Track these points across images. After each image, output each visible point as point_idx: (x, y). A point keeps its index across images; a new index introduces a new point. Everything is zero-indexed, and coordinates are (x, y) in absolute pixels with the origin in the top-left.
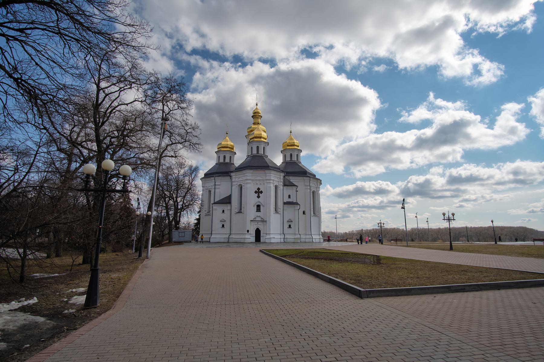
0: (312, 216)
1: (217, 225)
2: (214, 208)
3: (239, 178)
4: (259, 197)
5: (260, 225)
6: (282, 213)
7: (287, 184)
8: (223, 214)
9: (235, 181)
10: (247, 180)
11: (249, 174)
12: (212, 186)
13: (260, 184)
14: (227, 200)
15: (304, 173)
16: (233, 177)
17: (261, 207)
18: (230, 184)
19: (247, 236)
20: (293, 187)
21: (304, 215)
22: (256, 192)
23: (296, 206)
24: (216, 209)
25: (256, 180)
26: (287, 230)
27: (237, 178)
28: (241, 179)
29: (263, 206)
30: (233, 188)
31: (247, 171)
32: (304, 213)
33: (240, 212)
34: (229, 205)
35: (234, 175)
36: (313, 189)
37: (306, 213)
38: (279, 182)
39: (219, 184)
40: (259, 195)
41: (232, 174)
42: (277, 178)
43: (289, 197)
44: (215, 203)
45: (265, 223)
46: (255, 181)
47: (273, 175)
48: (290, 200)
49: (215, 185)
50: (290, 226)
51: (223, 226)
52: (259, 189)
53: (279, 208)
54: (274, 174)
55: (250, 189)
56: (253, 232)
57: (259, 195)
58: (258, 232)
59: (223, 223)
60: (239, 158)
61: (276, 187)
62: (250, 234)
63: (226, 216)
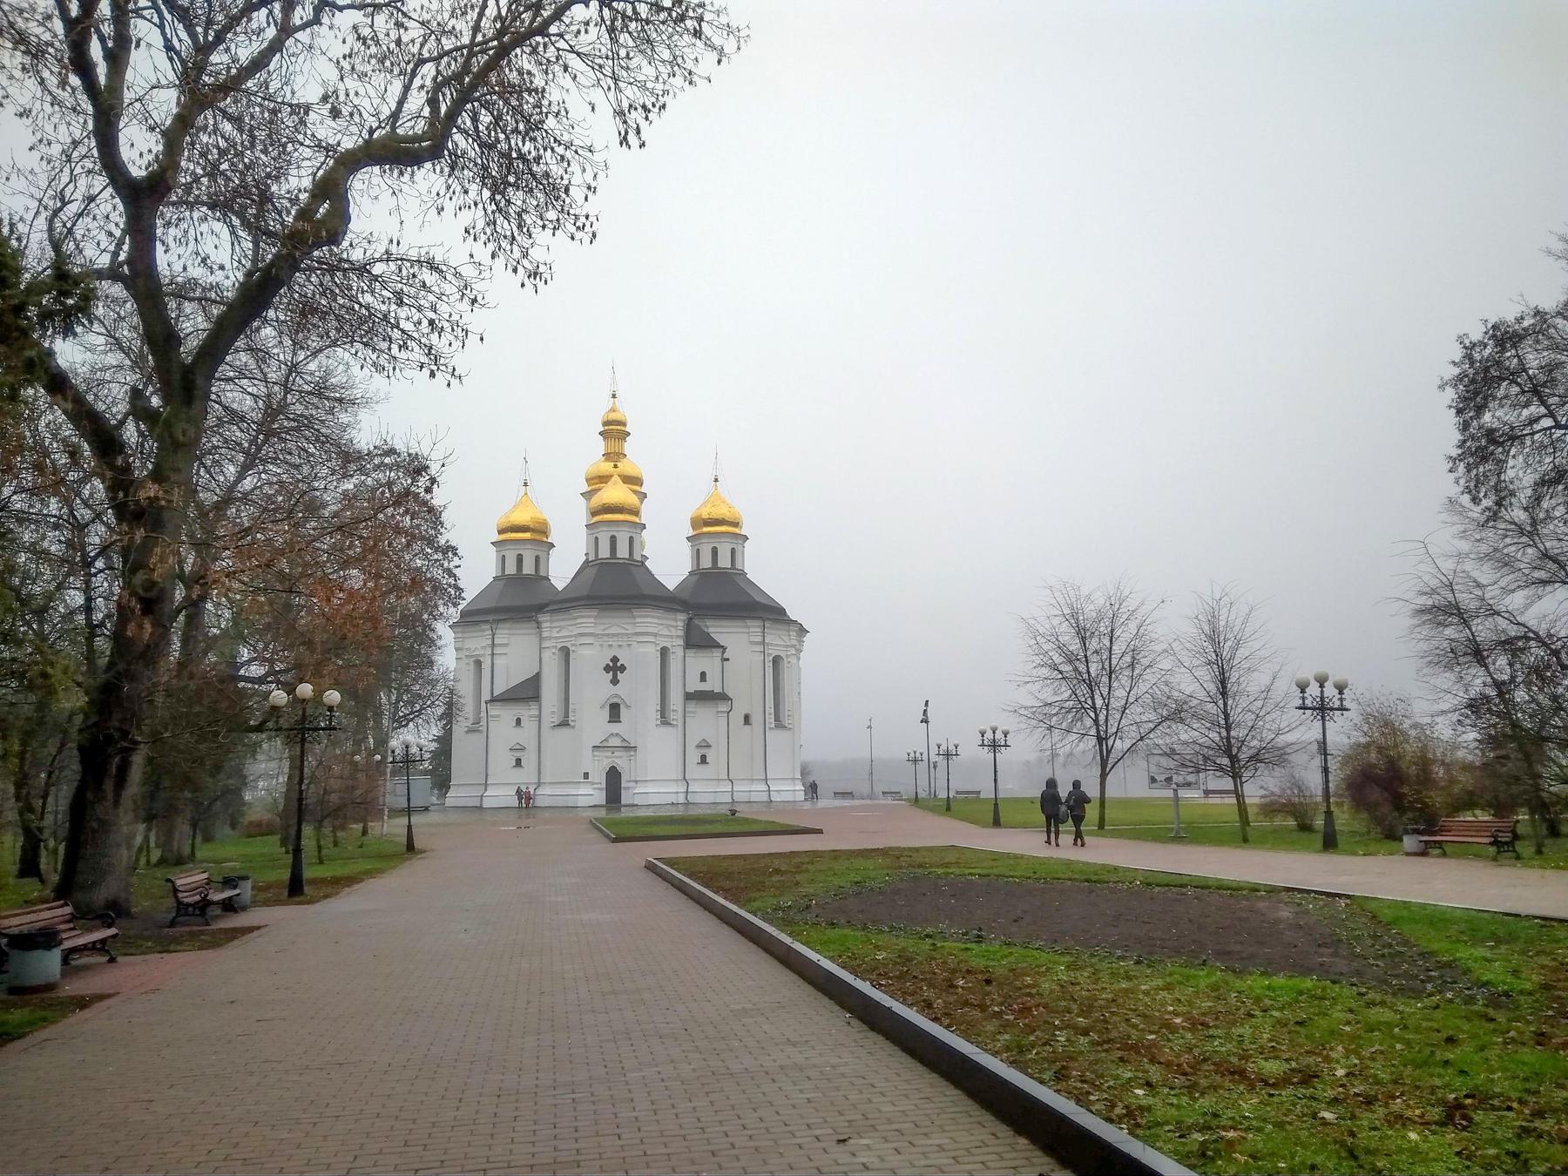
0: (770, 728)
1: (501, 761)
2: (491, 713)
3: (562, 628)
4: (615, 681)
5: (621, 757)
6: (680, 725)
7: (697, 641)
8: (518, 730)
9: (550, 638)
11: (586, 621)
12: (484, 648)
13: (620, 646)
14: (527, 692)
16: (544, 625)
17: (622, 708)
18: (534, 640)
19: (584, 790)
20: (713, 650)
22: (607, 669)
23: (719, 702)
24: (498, 716)
25: (608, 635)
26: (694, 770)
27: (557, 629)
28: (564, 633)
29: (628, 707)
30: (546, 655)
32: (747, 720)
33: (564, 724)
35: (547, 621)
37: (753, 719)
38: (672, 637)
39: (505, 641)
40: (615, 676)
41: (542, 618)
42: (668, 626)
43: (703, 676)
44: (494, 700)
45: (632, 753)
46: (606, 639)
47: (655, 621)
49: (493, 645)
50: (703, 760)
51: (518, 762)
52: (615, 659)
53: (673, 711)
54: (658, 618)
55: (590, 659)
56: (599, 777)
57: (615, 676)
58: (614, 776)
59: (518, 754)
60: (563, 568)
61: (664, 652)
62: (593, 783)
63: (526, 735)
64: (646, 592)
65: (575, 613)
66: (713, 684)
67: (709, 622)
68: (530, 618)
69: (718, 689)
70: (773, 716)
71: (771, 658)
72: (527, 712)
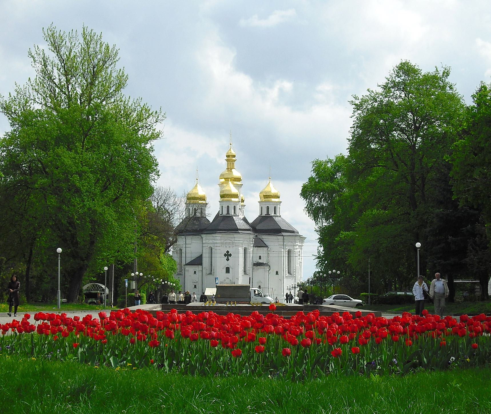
4: (228, 260)
7: (259, 244)
8: (195, 275)
10: (216, 243)
14: (198, 261)
15: (277, 231)
21: (277, 275)
22: (225, 255)
27: (208, 239)
32: (277, 273)
33: (211, 274)
34: (200, 267)
36: (288, 248)
40: (228, 257)
41: (203, 235)
43: (260, 257)
44: (186, 265)
51: (195, 286)
52: (228, 252)
57: (228, 257)
59: (195, 284)
60: (211, 214)
61: (245, 250)
65: (214, 235)
66: (263, 261)
67: (263, 237)
70: (287, 272)
71: (287, 250)
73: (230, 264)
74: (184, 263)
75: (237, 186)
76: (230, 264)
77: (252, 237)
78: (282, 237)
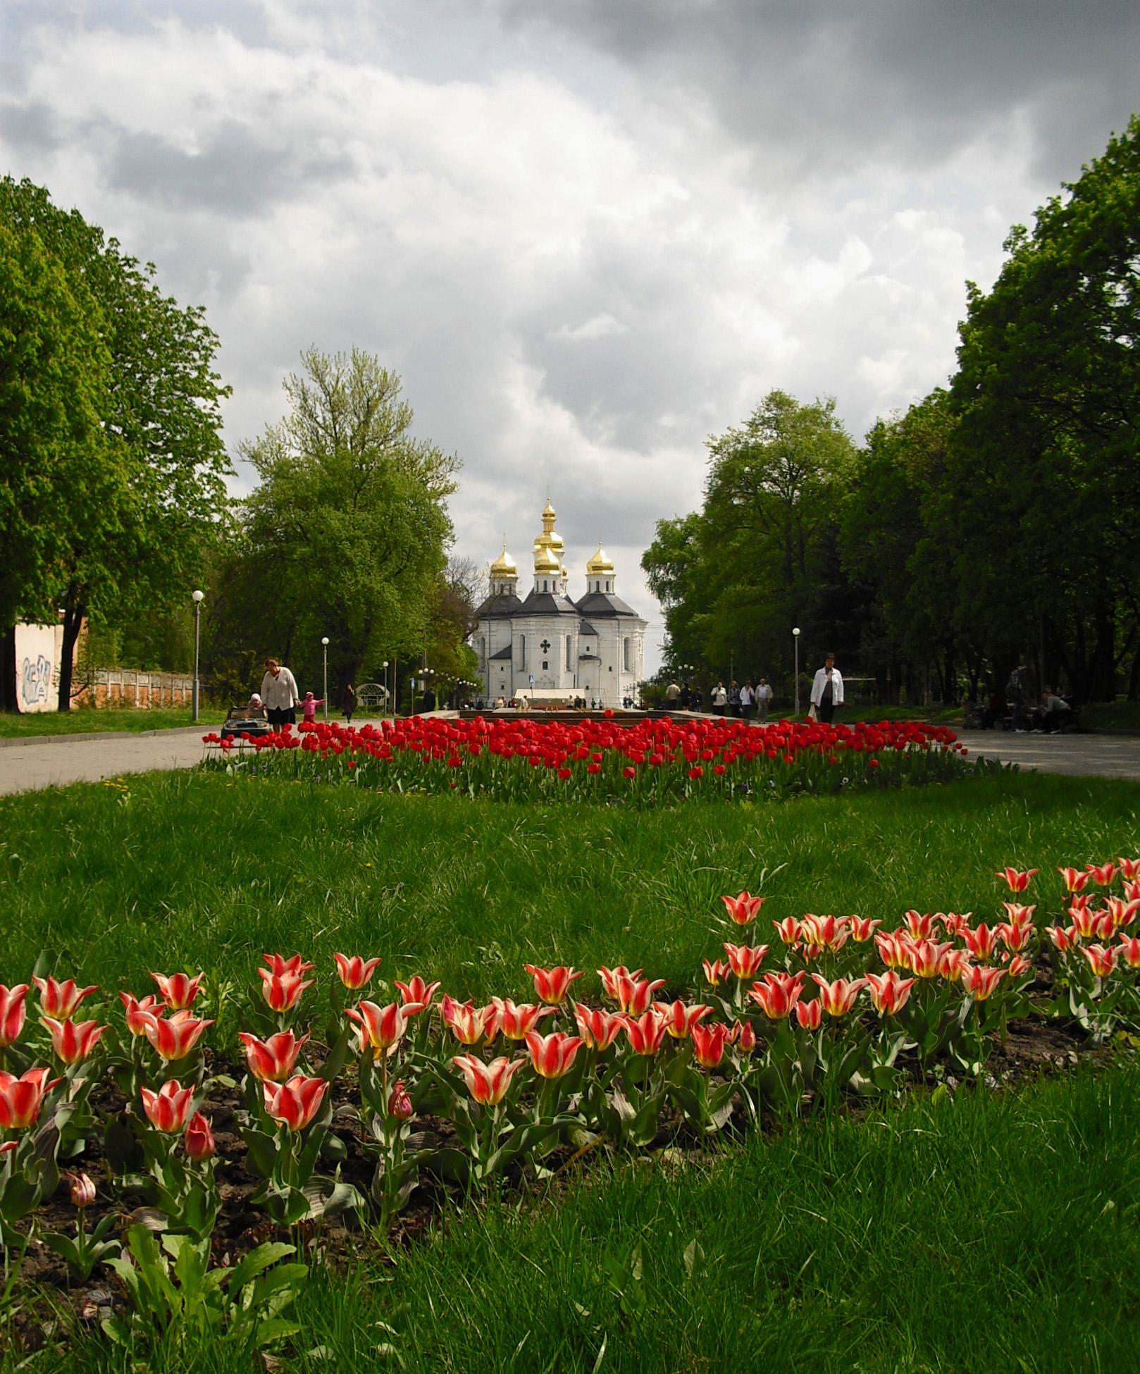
4: (545, 651)
7: (587, 631)
14: (506, 654)
22: (542, 646)
27: (520, 625)
31: (531, 619)
32: (610, 669)
33: (522, 670)
36: (625, 636)
43: (588, 649)
44: (491, 658)
48: (589, 653)
51: (503, 687)
52: (545, 641)
61: (568, 639)
63: (505, 675)
64: (560, 609)
65: (527, 619)
66: (592, 653)
68: (506, 619)
69: (595, 655)
72: (506, 663)
73: (548, 657)
74: (487, 656)
75: (560, 555)
76: (548, 657)
77: (577, 621)
78: (616, 622)
